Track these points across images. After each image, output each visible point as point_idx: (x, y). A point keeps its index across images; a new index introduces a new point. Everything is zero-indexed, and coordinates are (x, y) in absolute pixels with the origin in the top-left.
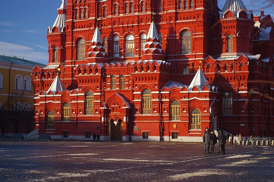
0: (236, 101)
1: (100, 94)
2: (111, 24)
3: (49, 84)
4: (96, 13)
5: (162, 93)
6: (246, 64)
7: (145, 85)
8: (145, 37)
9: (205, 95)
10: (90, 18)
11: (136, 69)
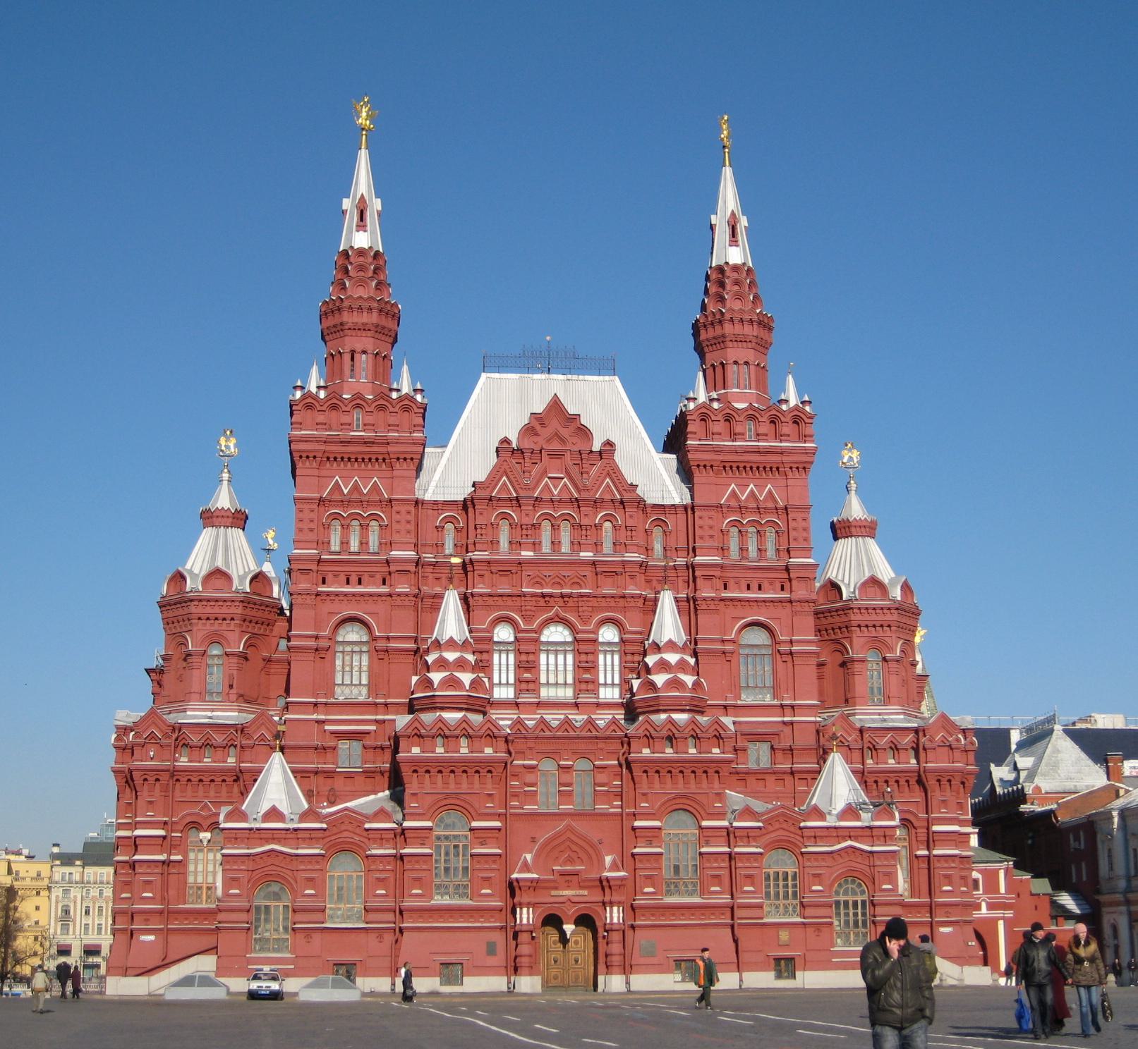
1: (497, 824)
3: (243, 780)
5: (735, 824)
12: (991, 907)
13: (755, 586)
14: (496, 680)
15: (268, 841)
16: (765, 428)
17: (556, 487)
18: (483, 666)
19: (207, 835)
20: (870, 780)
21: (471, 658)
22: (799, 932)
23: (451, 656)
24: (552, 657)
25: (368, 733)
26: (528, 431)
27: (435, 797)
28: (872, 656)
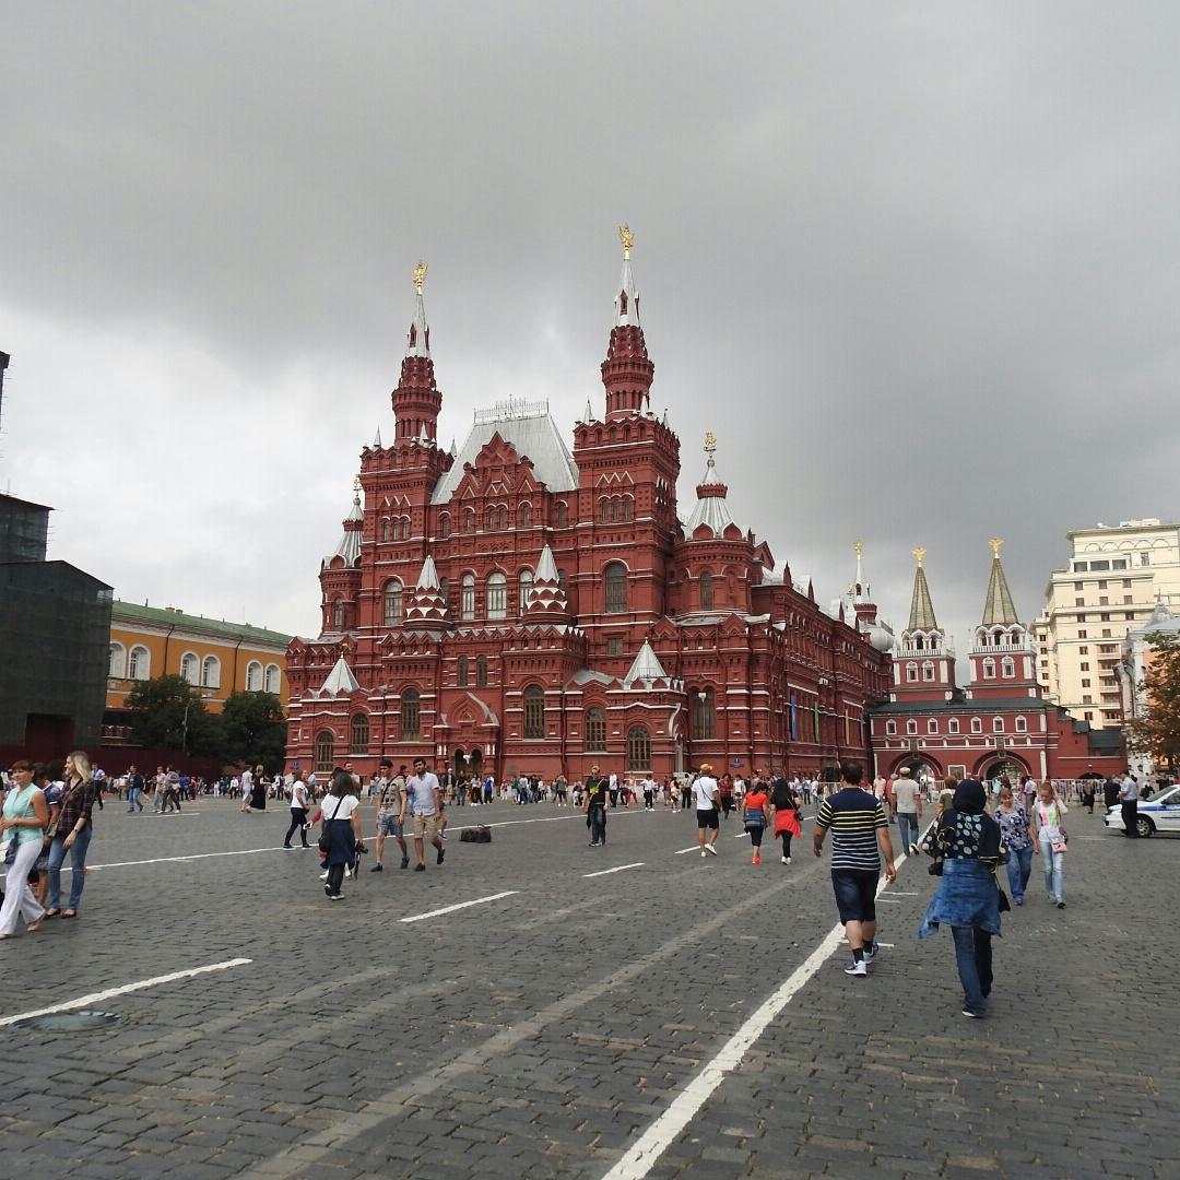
3: (325, 673)
7: (532, 676)
8: (526, 577)
11: (512, 642)
13: (615, 538)
18: (459, 601)
20: (686, 661)
22: (603, 761)
23: (419, 598)
27: (400, 682)
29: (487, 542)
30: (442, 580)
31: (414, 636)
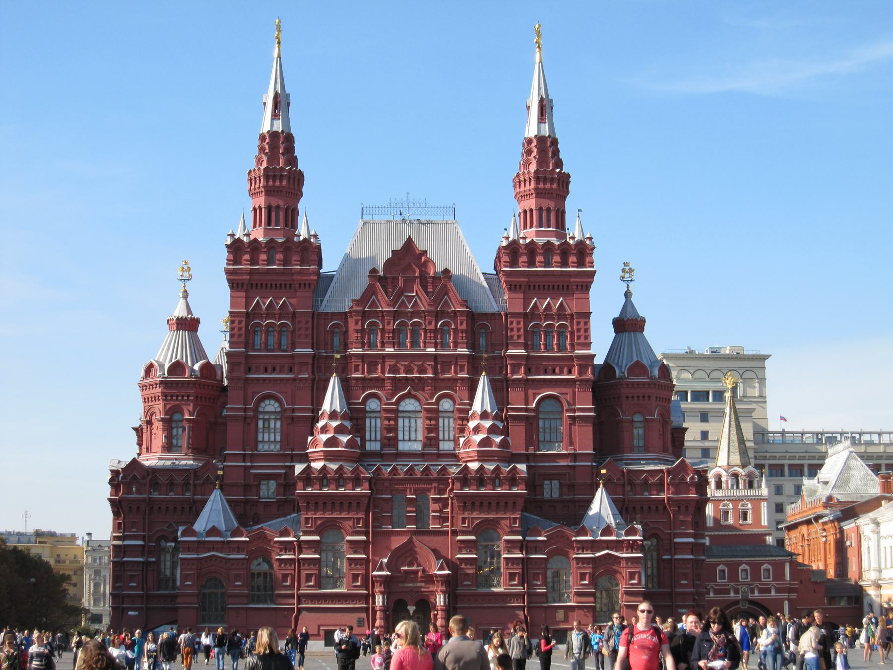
0: (670, 560)
1: (364, 538)
2: (360, 367)
3: (195, 509)
4: (313, 339)
5: (527, 538)
6: (692, 478)
9: (632, 546)
10: (298, 350)
12: (778, 590)
14: (368, 437)
15: (209, 551)
16: (557, 258)
17: (410, 303)
19: (173, 544)
21: (348, 424)
23: (335, 424)
24: (407, 421)
25: (280, 474)
26: (388, 264)
28: (638, 418)
29: (402, 365)
30: (349, 404)
31: (340, 468)
